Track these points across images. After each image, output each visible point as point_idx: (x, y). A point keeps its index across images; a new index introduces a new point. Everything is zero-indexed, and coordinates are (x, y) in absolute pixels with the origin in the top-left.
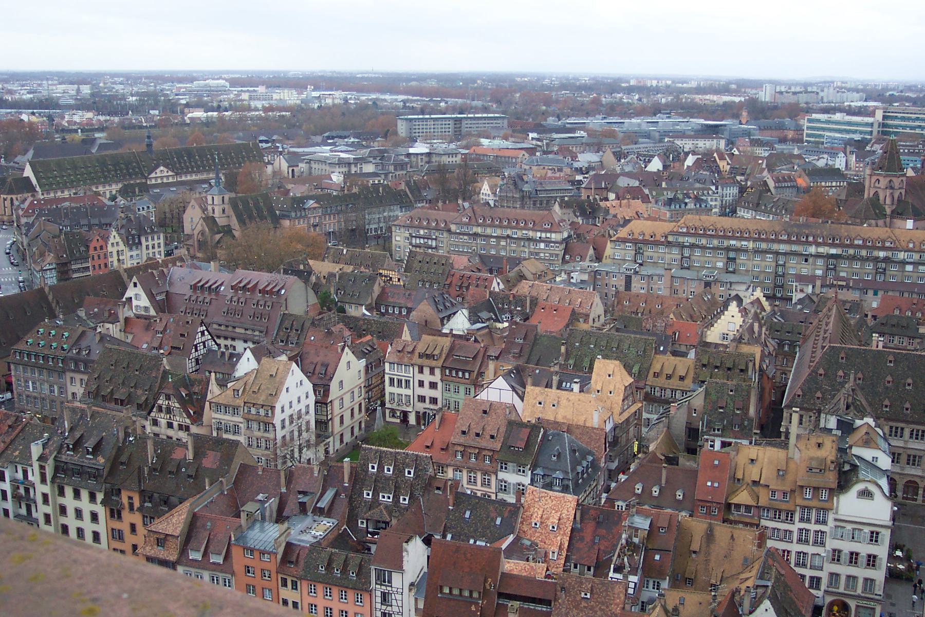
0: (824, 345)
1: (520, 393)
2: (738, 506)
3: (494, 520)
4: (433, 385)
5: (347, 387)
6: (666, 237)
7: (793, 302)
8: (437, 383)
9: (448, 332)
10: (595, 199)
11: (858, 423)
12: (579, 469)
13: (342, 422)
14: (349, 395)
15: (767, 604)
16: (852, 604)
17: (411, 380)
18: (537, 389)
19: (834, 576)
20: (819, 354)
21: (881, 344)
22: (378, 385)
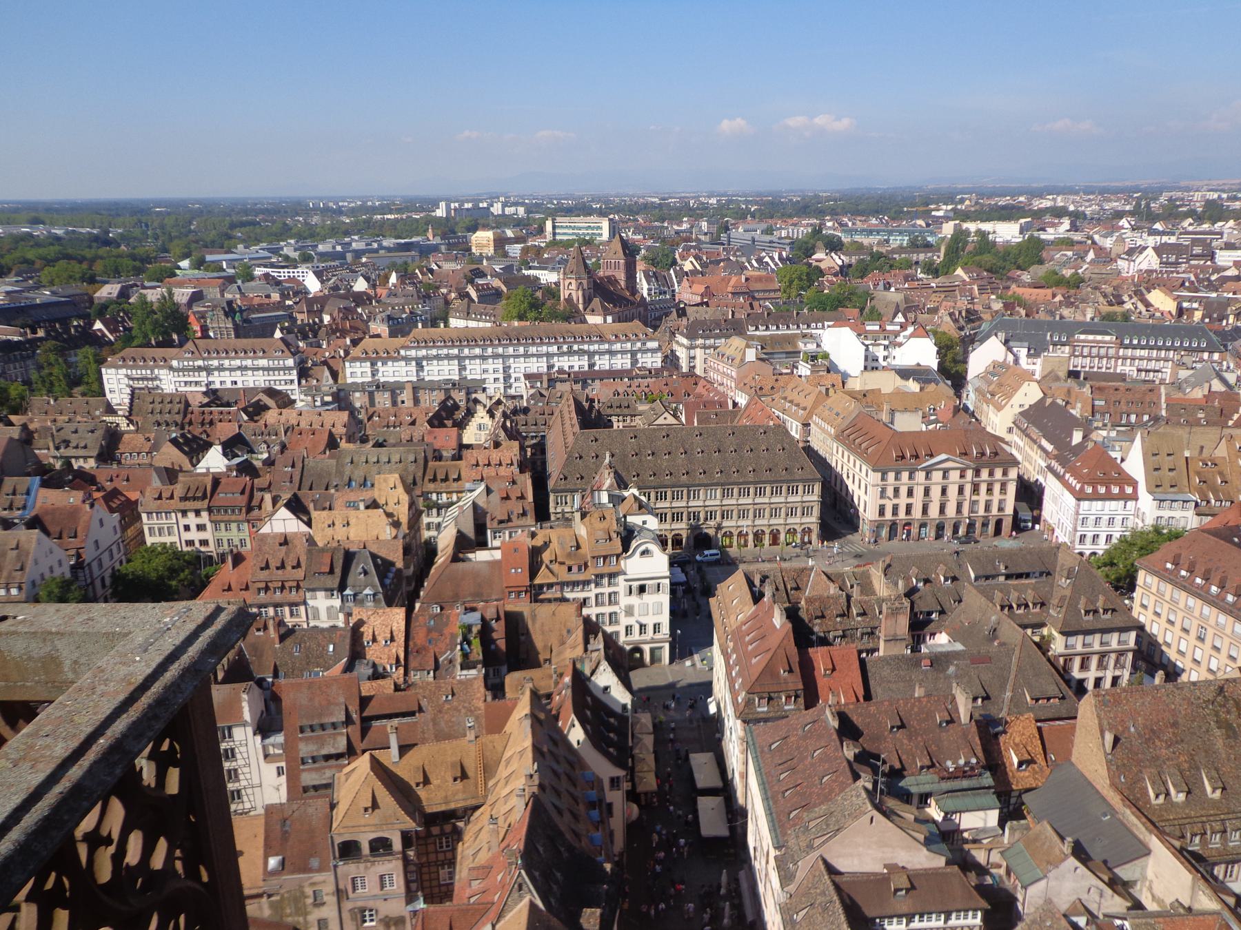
0: (575, 430)
1: (305, 519)
2: (541, 586)
3: (325, 648)
4: (201, 528)
5: (103, 546)
6: (399, 353)
7: (525, 398)
8: (205, 525)
9: (204, 471)
10: (314, 321)
11: (626, 494)
12: (388, 581)
13: (104, 586)
14: (107, 554)
15: (604, 665)
16: (646, 648)
17: (175, 526)
18: (325, 513)
19: (628, 629)
20: (571, 439)
21: (621, 424)
22: (135, 538)
